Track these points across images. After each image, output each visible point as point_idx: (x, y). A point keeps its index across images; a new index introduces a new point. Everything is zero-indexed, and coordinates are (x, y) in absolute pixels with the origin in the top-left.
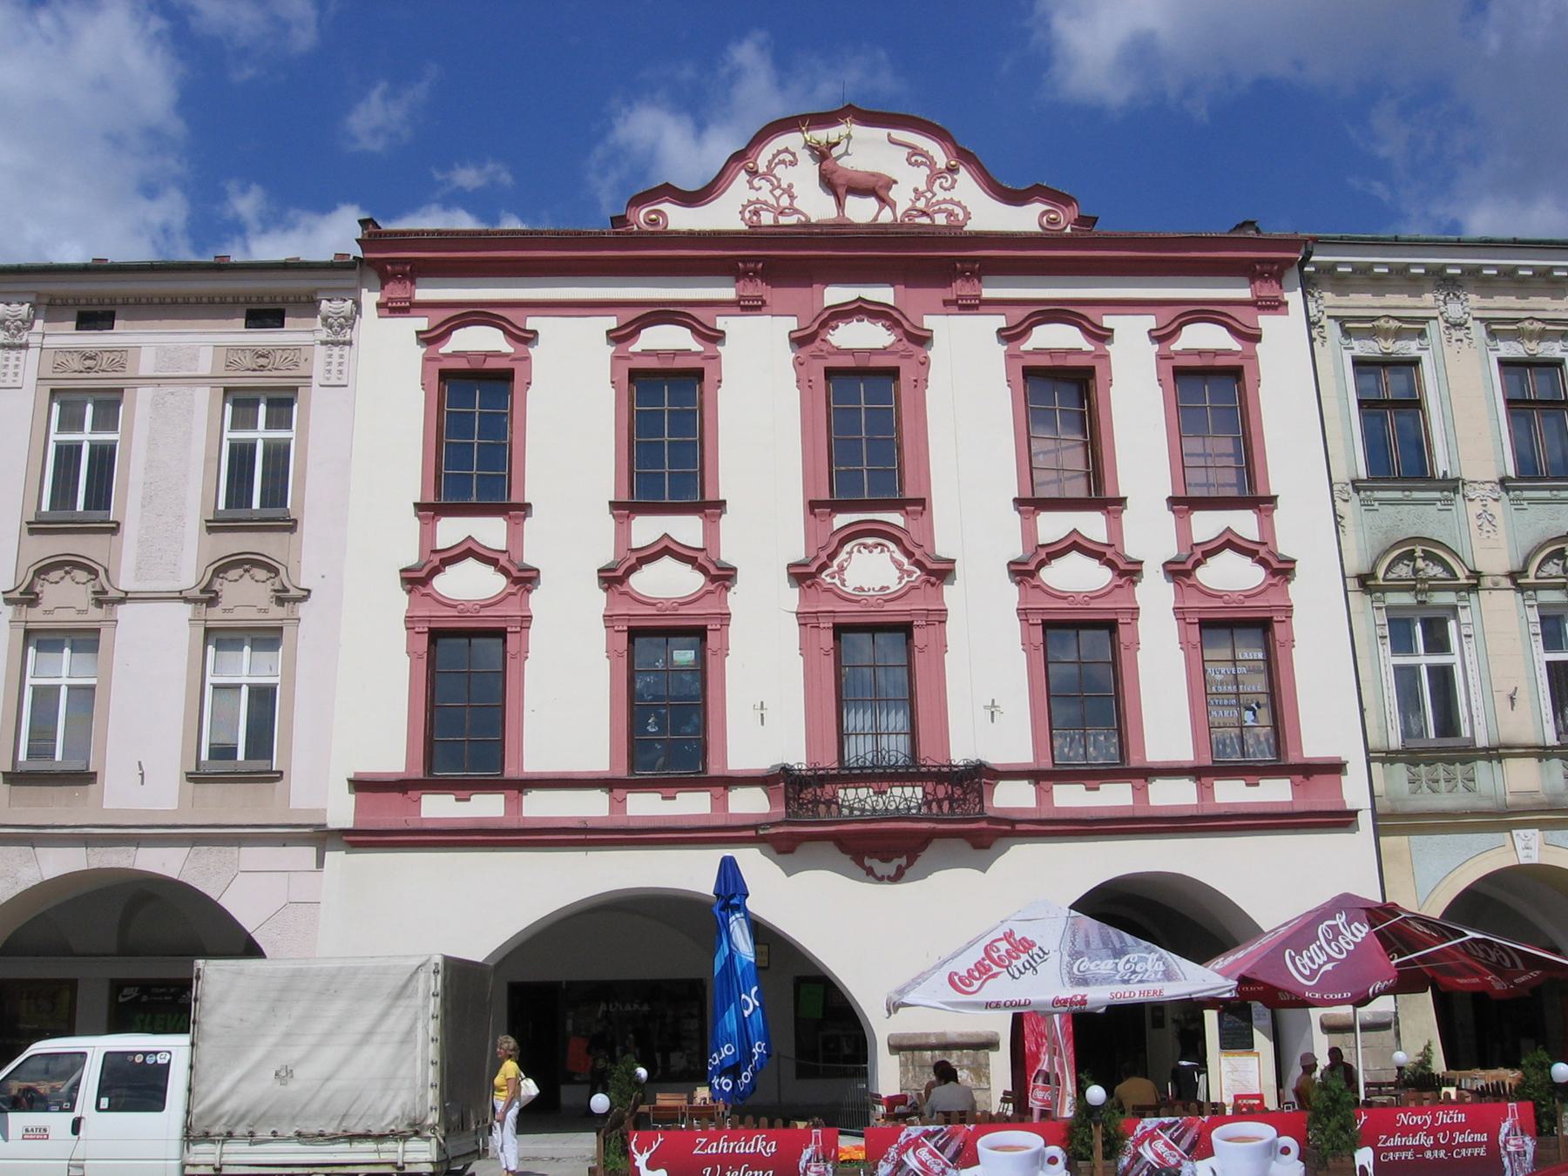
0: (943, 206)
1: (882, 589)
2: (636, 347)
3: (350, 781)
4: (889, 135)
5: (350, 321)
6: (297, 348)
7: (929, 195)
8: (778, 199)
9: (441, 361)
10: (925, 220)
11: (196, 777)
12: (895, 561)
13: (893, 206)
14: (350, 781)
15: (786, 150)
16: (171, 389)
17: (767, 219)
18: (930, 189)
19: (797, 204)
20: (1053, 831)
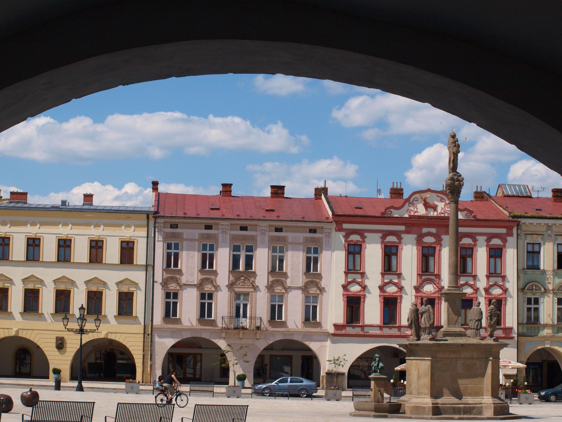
0: (447, 212)
1: (430, 291)
3: (333, 324)
4: (437, 195)
5: (330, 233)
7: (444, 209)
8: (414, 209)
10: (443, 215)
12: (433, 286)
13: (437, 212)
14: (333, 324)
15: (416, 198)
17: (412, 213)
18: (445, 208)
19: (418, 210)
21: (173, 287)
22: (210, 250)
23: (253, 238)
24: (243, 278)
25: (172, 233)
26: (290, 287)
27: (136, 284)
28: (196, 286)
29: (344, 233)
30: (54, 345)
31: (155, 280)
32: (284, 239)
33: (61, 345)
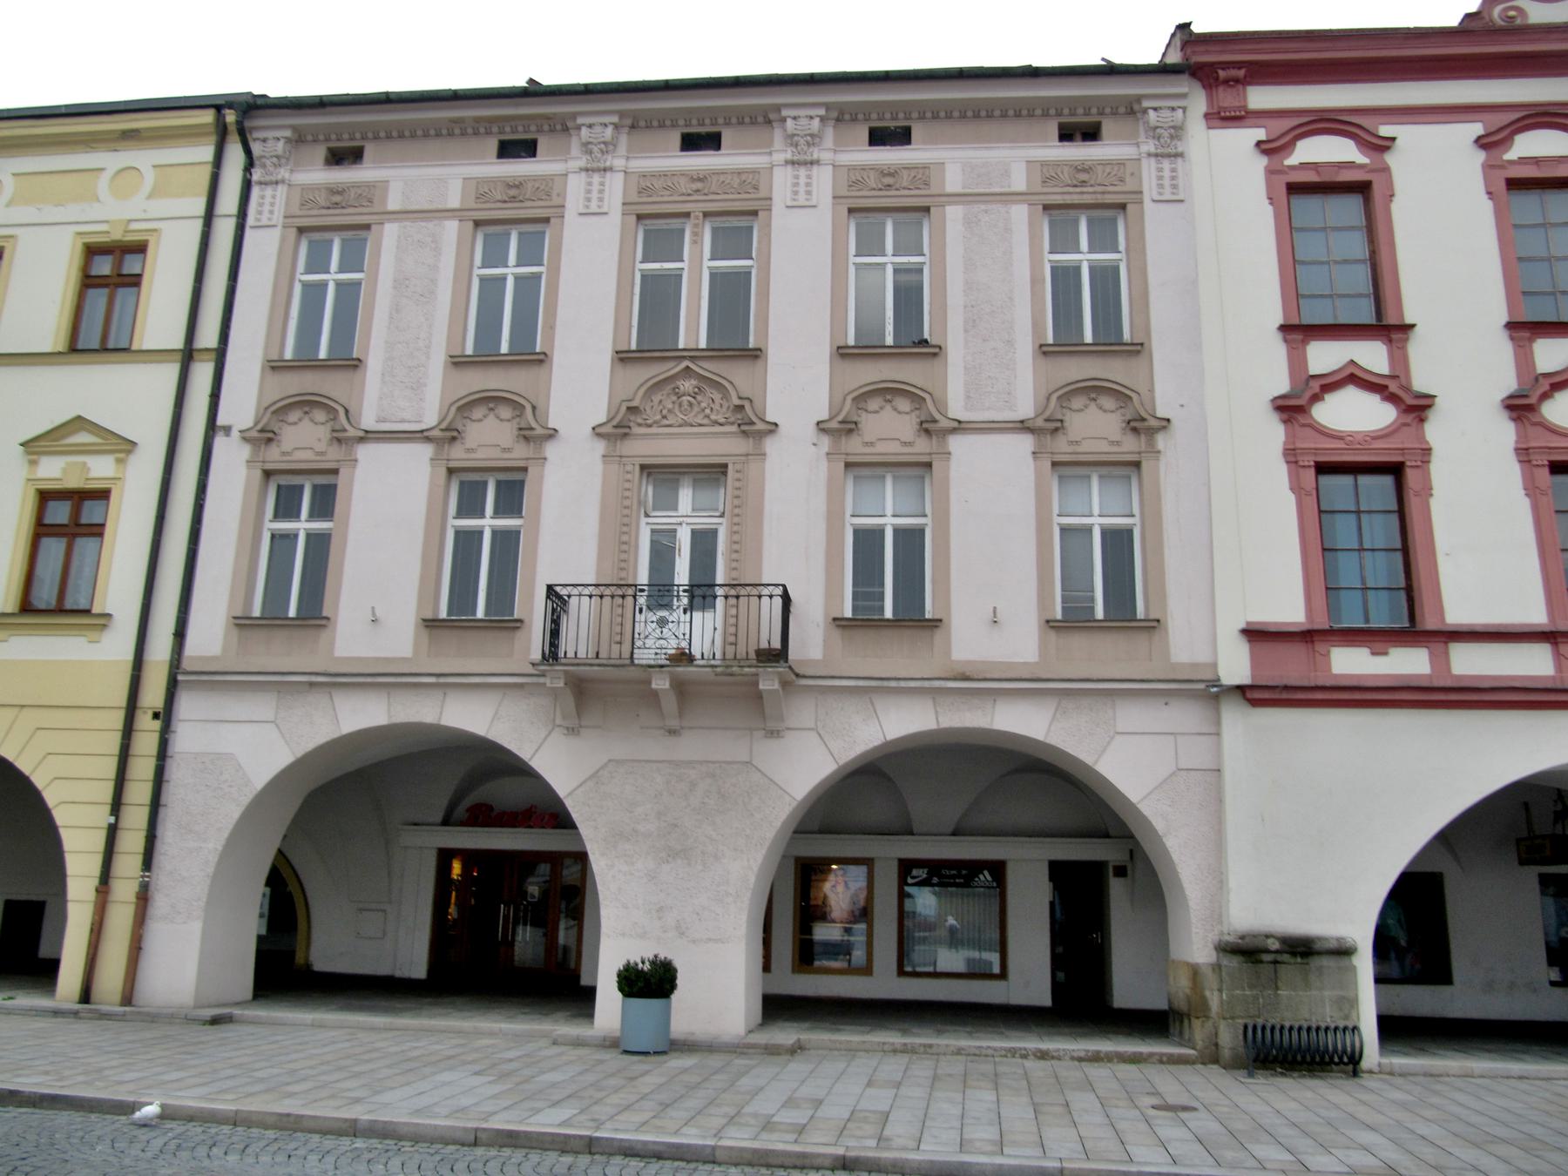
5: (1177, 131)
6: (1121, 163)
9: (1287, 174)
16: (983, 207)
20: (1423, 701)
23: (751, 181)
24: (687, 385)
25: (334, 190)
26: (960, 427)
27: (124, 447)
28: (428, 439)
31: (222, 420)
32: (922, 175)
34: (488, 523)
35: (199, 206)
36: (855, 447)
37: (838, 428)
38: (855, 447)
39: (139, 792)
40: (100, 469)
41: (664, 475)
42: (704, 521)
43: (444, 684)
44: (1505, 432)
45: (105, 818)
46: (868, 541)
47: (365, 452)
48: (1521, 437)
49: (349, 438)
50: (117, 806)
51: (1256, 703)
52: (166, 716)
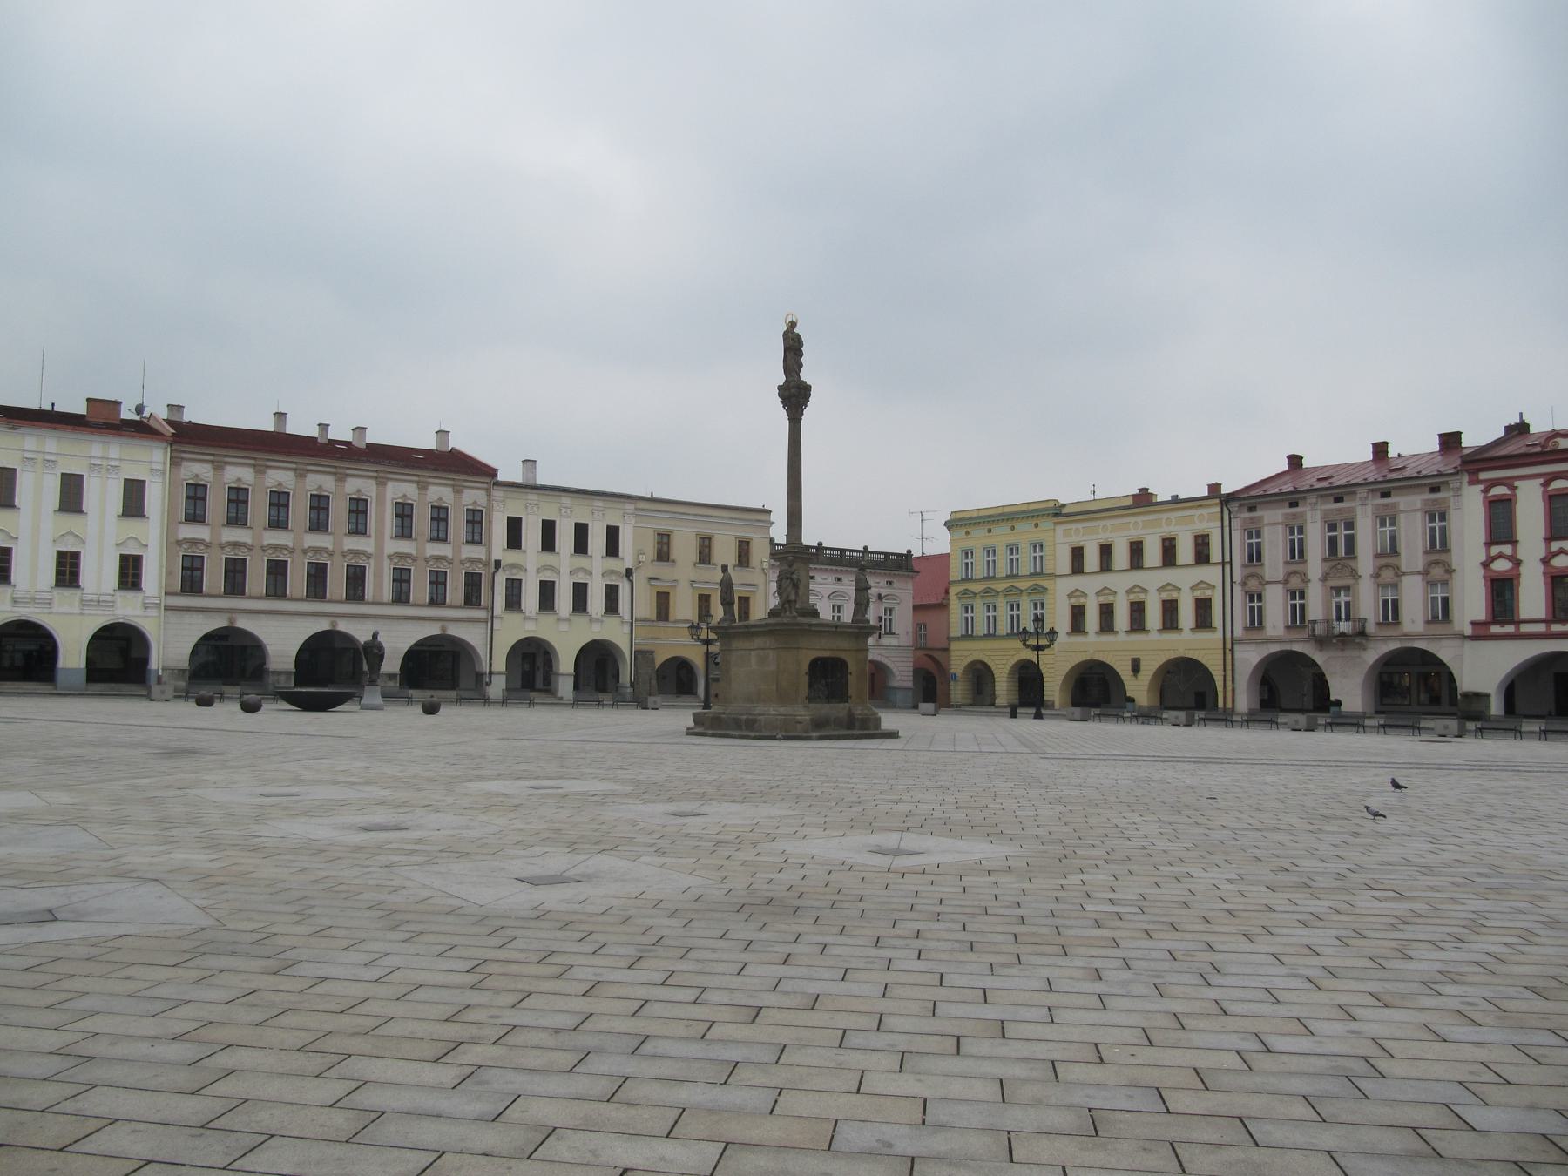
2: (1550, 488)
6: (1445, 498)
11: (1428, 622)
21: (1253, 585)
22: (1298, 534)
23: (1352, 510)
24: (1339, 567)
25: (1251, 519)
26: (1404, 574)
29: (1481, 487)
30: (1130, 668)
32: (1394, 505)
33: (1136, 666)
34: (1298, 602)
35: (1220, 525)
36: (1380, 580)
37: (1376, 576)
38: (1380, 580)
39: (1229, 667)
40: (1208, 593)
41: (1337, 590)
42: (1348, 599)
43: (1291, 641)
44: (1541, 568)
45: (1223, 673)
46: (1385, 602)
47: (1267, 586)
48: (1544, 570)
49: (1264, 583)
50: (1225, 670)
51: (1473, 640)
52: (1232, 650)
